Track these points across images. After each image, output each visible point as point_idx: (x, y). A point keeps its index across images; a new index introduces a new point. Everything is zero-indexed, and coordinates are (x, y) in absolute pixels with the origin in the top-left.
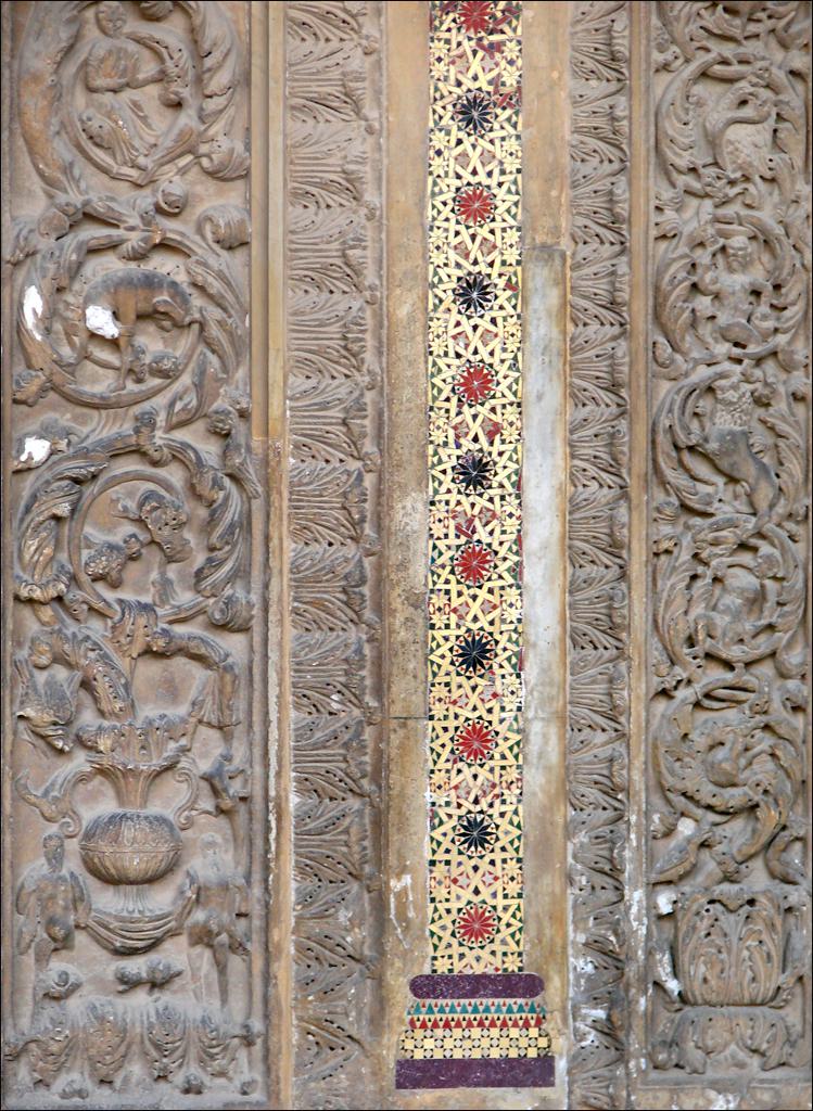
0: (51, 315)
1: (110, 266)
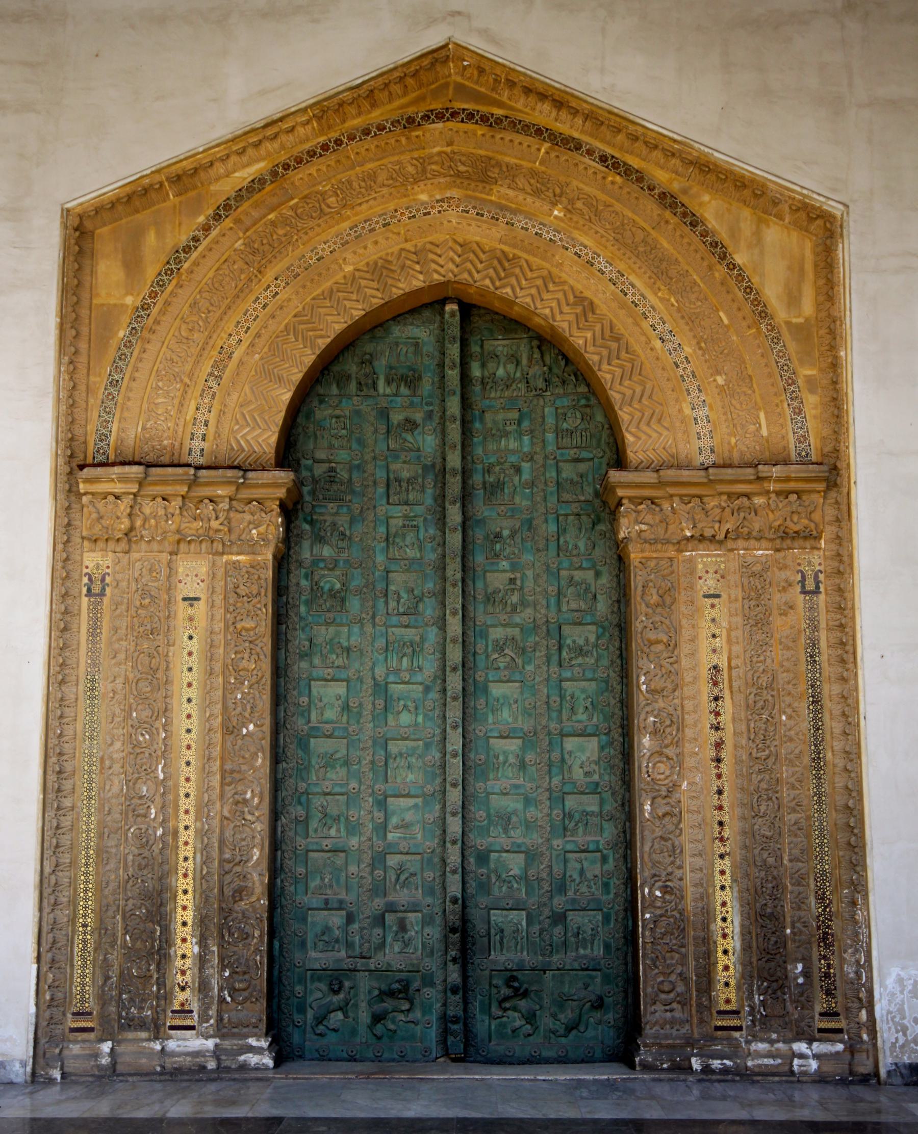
0: (650, 892)
1: (660, 884)
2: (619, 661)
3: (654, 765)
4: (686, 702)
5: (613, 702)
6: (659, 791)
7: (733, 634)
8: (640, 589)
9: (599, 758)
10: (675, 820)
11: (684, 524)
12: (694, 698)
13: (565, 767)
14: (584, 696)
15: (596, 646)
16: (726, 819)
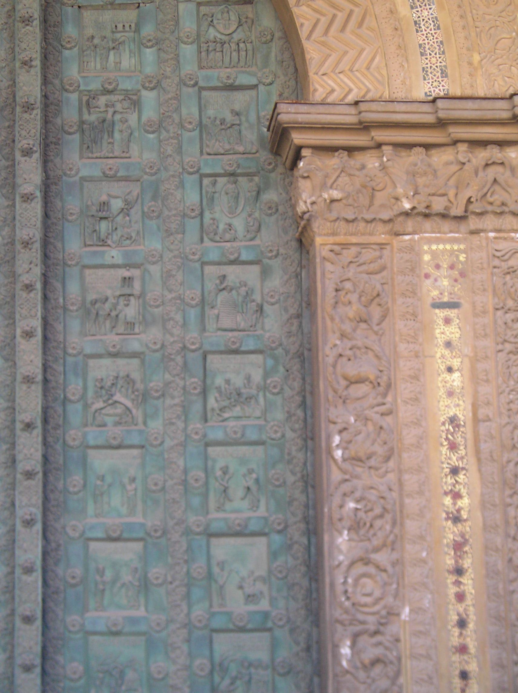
2: (300, 413)
3: (356, 581)
4: (406, 477)
5: (291, 479)
6: (363, 623)
7: (480, 366)
8: (331, 293)
9: (270, 572)
10: (391, 670)
11: (400, 190)
12: (419, 470)
13: (214, 586)
14: (244, 470)
15: (264, 388)
16: (472, 667)
